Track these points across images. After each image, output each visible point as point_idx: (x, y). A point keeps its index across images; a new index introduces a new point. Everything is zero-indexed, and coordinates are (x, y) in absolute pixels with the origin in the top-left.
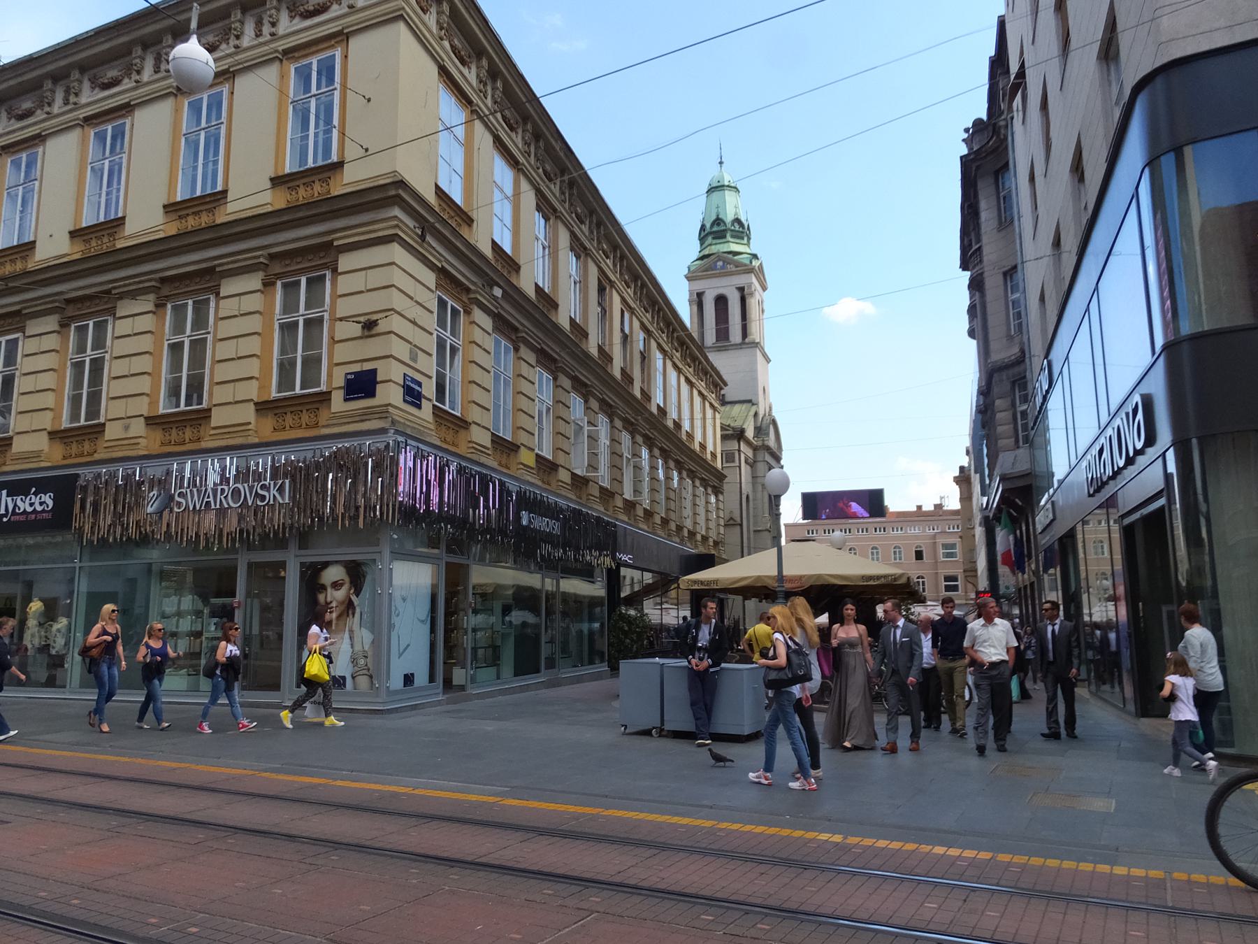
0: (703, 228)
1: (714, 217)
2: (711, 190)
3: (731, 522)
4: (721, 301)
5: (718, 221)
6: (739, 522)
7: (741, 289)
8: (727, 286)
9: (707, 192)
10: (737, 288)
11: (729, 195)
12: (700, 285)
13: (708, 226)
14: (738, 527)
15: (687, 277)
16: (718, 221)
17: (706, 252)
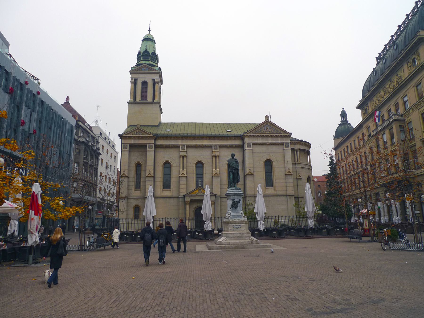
0: (139, 53)
2: (144, 40)
4: (145, 83)
5: (146, 51)
6: (153, 176)
7: (154, 80)
8: (148, 78)
12: (136, 76)
13: (142, 52)
14: (153, 178)
15: (131, 73)
16: (146, 51)
17: (139, 63)
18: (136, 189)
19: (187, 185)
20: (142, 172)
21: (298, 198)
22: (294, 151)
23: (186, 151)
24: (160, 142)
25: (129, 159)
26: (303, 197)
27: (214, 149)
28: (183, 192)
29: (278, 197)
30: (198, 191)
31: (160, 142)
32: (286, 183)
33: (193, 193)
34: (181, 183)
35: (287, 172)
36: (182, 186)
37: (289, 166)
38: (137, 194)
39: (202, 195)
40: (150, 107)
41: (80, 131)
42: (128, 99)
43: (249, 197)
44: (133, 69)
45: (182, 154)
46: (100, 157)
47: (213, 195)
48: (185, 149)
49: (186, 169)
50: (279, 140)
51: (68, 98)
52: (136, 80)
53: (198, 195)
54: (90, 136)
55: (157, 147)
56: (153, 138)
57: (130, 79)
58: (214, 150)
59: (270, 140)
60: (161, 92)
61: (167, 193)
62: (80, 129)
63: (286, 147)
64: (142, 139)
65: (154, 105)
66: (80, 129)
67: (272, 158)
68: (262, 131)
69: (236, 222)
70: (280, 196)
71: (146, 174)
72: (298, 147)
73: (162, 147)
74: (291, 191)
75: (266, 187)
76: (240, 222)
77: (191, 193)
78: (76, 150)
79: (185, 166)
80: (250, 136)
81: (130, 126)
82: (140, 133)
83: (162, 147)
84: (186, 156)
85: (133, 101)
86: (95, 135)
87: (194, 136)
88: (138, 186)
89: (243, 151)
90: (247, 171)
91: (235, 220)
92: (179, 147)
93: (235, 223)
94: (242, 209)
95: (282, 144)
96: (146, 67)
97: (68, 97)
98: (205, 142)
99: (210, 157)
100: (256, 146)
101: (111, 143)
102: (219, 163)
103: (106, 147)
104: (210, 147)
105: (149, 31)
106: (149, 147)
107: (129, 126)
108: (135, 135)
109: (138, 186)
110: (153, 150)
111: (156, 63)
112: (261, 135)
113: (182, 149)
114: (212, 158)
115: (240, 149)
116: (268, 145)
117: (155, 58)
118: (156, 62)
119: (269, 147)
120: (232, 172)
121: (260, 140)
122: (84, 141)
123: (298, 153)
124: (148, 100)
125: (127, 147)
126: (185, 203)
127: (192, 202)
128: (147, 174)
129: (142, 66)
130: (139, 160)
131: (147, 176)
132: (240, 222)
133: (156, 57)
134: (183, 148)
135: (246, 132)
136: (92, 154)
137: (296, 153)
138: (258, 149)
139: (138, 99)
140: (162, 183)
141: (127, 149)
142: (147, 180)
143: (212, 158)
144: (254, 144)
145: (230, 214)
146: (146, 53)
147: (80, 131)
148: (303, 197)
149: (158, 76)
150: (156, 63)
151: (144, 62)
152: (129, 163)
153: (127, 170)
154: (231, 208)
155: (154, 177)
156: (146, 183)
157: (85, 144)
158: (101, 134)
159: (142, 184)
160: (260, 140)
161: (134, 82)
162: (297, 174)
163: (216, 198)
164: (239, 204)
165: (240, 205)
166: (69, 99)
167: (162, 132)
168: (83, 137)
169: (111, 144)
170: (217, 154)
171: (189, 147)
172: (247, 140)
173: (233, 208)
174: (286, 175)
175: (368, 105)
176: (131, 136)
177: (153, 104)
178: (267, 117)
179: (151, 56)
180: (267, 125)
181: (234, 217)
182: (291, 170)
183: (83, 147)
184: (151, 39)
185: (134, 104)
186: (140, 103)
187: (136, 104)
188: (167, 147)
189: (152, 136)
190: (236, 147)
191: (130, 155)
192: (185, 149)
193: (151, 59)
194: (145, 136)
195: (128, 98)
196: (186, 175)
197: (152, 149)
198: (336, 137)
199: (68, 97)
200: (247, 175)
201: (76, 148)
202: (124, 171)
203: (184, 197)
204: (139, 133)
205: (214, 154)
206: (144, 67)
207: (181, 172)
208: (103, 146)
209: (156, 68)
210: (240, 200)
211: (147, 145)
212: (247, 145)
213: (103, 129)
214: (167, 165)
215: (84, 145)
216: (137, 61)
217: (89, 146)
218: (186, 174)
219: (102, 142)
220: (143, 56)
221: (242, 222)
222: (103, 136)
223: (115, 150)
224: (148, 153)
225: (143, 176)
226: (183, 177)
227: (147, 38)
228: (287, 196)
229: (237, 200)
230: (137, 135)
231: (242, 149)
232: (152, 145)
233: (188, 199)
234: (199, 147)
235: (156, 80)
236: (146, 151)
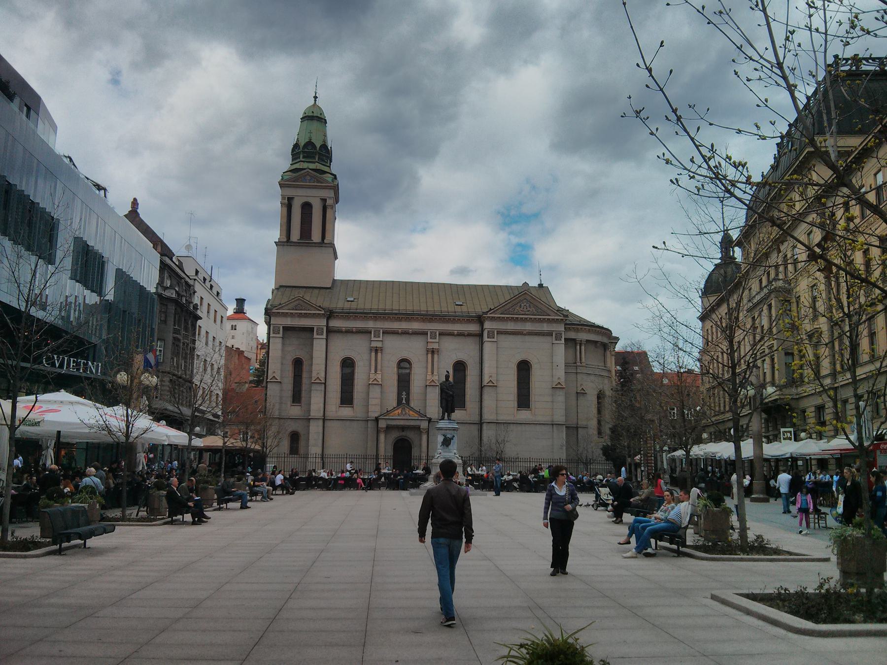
0: (296, 146)
1: (307, 140)
3: (318, 381)
4: (307, 207)
5: (310, 144)
8: (314, 197)
12: (290, 192)
13: (302, 144)
14: (323, 385)
16: (310, 144)
17: (297, 166)
18: (293, 402)
19: (382, 399)
20: (305, 375)
21: (577, 428)
22: (576, 344)
24: (335, 323)
25: (283, 350)
26: (587, 428)
27: (431, 338)
28: (374, 412)
29: (538, 427)
30: (400, 411)
31: (335, 323)
32: (552, 402)
33: (391, 414)
35: (556, 383)
36: (372, 402)
37: (560, 373)
38: (295, 411)
40: (316, 251)
44: (285, 178)
45: (374, 344)
46: (199, 322)
47: (426, 418)
48: (379, 337)
50: (545, 327)
51: (135, 203)
52: (290, 199)
55: (330, 331)
58: (429, 340)
59: (529, 327)
61: (346, 412)
63: (556, 340)
67: (529, 358)
68: (516, 311)
71: (311, 378)
72: (583, 336)
73: (339, 331)
74: (560, 417)
79: (379, 367)
81: (281, 286)
83: (339, 331)
84: (381, 349)
85: (285, 240)
86: (188, 276)
87: (396, 314)
88: (297, 398)
90: (486, 380)
94: (456, 448)
95: (550, 334)
96: (309, 176)
97: (135, 200)
98: (416, 326)
99: (424, 352)
101: (213, 289)
102: (438, 361)
103: (208, 299)
104: (424, 333)
105: (316, 97)
107: (280, 288)
108: (293, 309)
109: (297, 398)
110: (324, 336)
111: (328, 165)
113: (374, 337)
114: (427, 354)
115: (477, 339)
116: (525, 335)
118: (327, 162)
121: (510, 326)
122: (174, 296)
123: (583, 347)
126: (378, 432)
127: (389, 428)
130: (299, 354)
133: (329, 153)
134: (377, 335)
135: (488, 312)
137: (578, 347)
138: (506, 342)
139: (295, 236)
140: (339, 395)
143: (427, 354)
144: (500, 333)
146: (310, 147)
148: (587, 428)
149: (331, 194)
151: (305, 165)
152: (283, 358)
153: (279, 372)
155: (325, 384)
157: (176, 302)
158: (197, 272)
159: (304, 394)
160: (510, 326)
161: (288, 204)
162: (579, 385)
163: (431, 423)
167: (339, 304)
169: (215, 291)
170: (436, 346)
172: (487, 325)
175: (750, 244)
179: (319, 154)
182: (562, 380)
183: (172, 308)
184: (319, 116)
185: (288, 245)
188: (349, 332)
189: (323, 312)
190: (470, 335)
191: (283, 344)
192: (379, 337)
195: (276, 234)
198: (706, 292)
199: (135, 200)
203: (377, 420)
205: (430, 346)
206: (306, 176)
208: (202, 298)
209: (329, 178)
210: (454, 436)
213: (200, 260)
214: (348, 364)
216: (293, 160)
218: (380, 380)
219: (200, 291)
222: (201, 276)
223: (220, 302)
224: (315, 342)
225: (305, 381)
226: (375, 386)
227: (311, 114)
228: (553, 425)
229: (449, 436)
230: (296, 310)
232: (323, 329)
233: (382, 424)
234: (405, 333)
235: (329, 202)
236: (313, 339)
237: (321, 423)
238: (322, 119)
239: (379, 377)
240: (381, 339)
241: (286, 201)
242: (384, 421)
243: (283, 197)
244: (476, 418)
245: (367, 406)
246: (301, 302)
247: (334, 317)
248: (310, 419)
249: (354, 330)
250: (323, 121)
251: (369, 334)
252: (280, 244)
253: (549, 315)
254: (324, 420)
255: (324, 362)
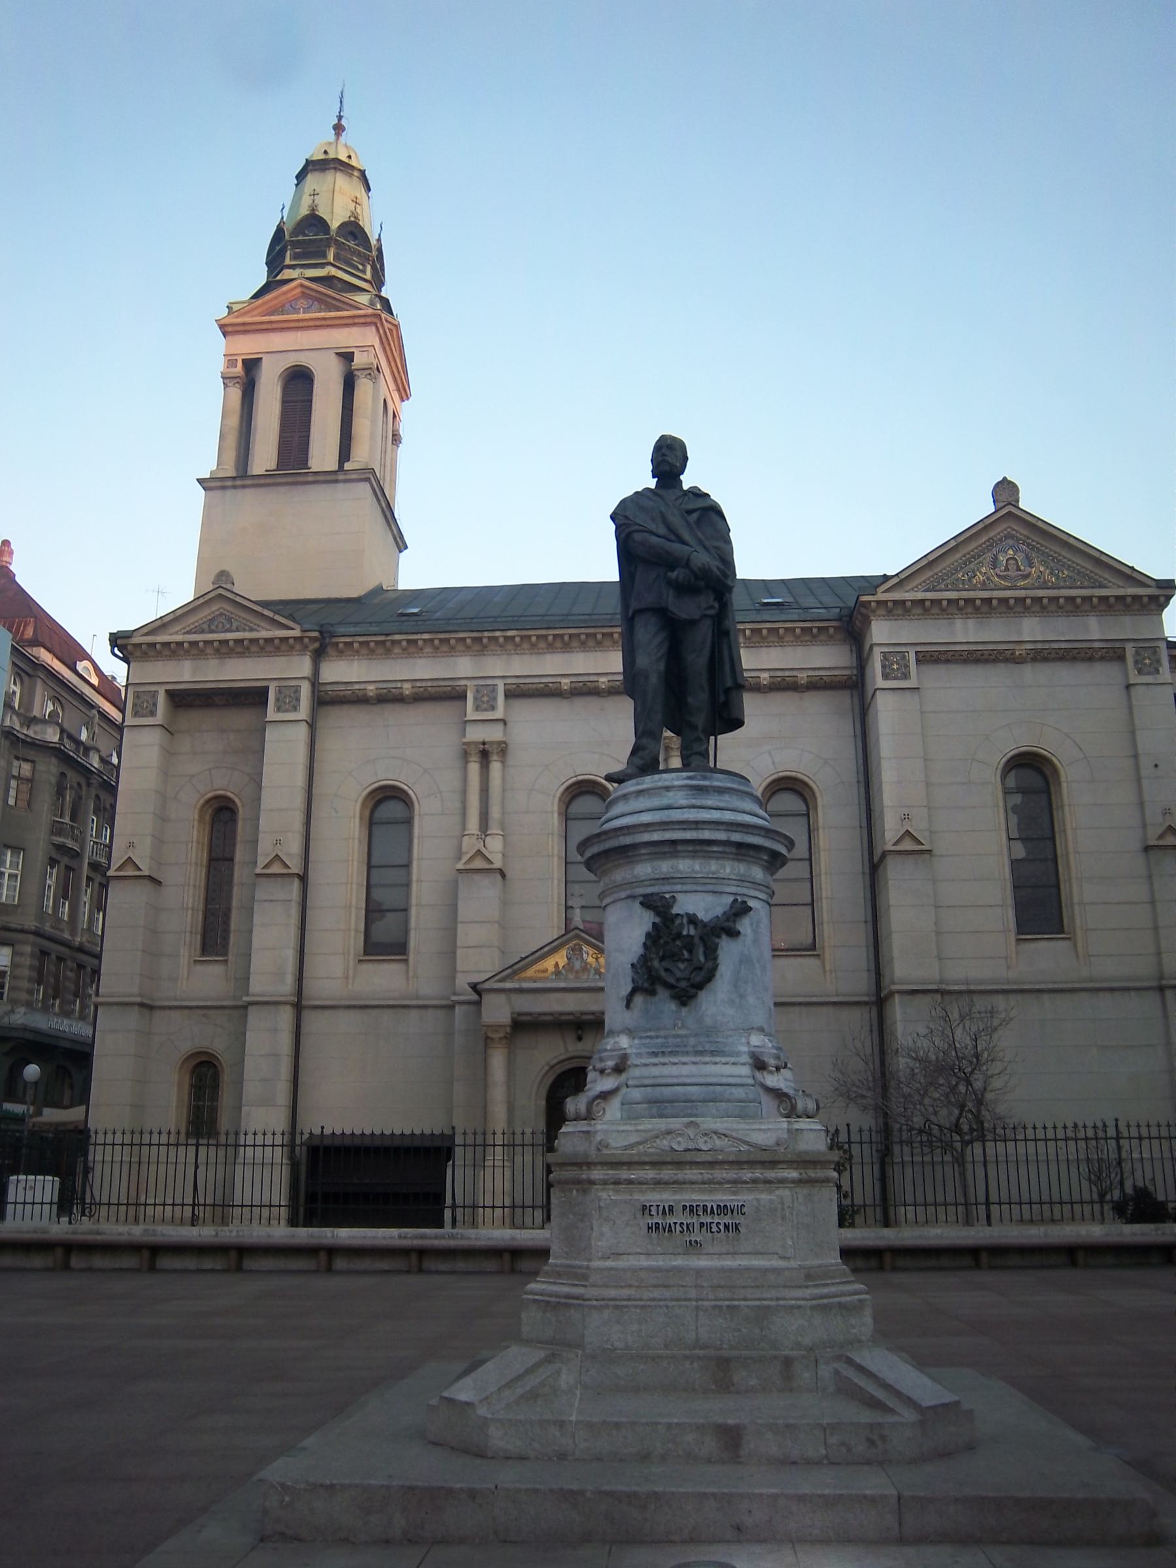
0: (279, 233)
2: (311, 167)
3: (276, 869)
7: (347, 357)
9: (297, 177)
10: (336, 353)
11: (343, 184)
12: (249, 345)
14: (296, 884)
15: (226, 329)
16: (314, 221)
20: (240, 854)
23: (504, 722)
25: (165, 773)
33: (530, 972)
34: (463, 912)
35: (1160, 830)
36: (468, 935)
39: (593, 985)
40: (319, 495)
41: (39, 690)
42: (208, 465)
43: (907, 998)
44: (236, 307)
45: (476, 734)
48: (493, 708)
49: (503, 825)
52: (252, 365)
53: (562, 985)
54: (97, 719)
56: (306, 647)
57: (220, 365)
60: (396, 439)
62: (39, 683)
64: (241, 655)
65: (340, 486)
66: (39, 683)
69: (679, 1164)
70: (1112, 990)
73: (355, 699)
75: (1019, 933)
76: (737, 1164)
77: (515, 969)
78: (13, 783)
79: (495, 812)
80: (898, 610)
82: (229, 620)
83: (355, 699)
84: (503, 749)
89: (857, 709)
90: (890, 829)
91: (665, 1143)
92: (459, 696)
93: (667, 1174)
100: (941, 670)
105: (339, 129)
106: (277, 700)
108: (203, 632)
110: (303, 712)
112: (970, 601)
113: (477, 708)
115: (844, 699)
117: (359, 254)
118: (364, 272)
119: (1028, 672)
120: (662, 612)
124: (310, 464)
125: (155, 705)
128: (262, 861)
129: (285, 293)
131: (258, 870)
132: (737, 1164)
136: (105, 809)
141: (153, 713)
142: (260, 894)
144: (930, 657)
145: (619, 1069)
147: (39, 690)
149: (369, 336)
150: (368, 276)
153: (148, 841)
154: (639, 999)
155: (303, 878)
156: (257, 919)
164: (728, 950)
165: (745, 960)
166: (11, 553)
168: (53, 719)
171: (516, 693)
172: (881, 632)
173: (652, 992)
174: (1147, 849)
176: (179, 638)
177: (336, 481)
178: (1005, 491)
179: (336, 242)
180: (1009, 536)
181: (660, 1106)
184: (346, 160)
185: (234, 487)
186: (268, 481)
187: (244, 487)
188: (389, 698)
189: (297, 633)
190: (817, 685)
191: (169, 754)
192: (493, 708)
193: (336, 257)
194: (254, 635)
196: (498, 864)
197: (295, 708)
200: (884, 855)
201: (14, 777)
202: (131, 845)
204: (222, 619)
207: (470, 845)
210: (740, 910)
211: (267, 688)
212: (884, 667)
215: (54, 760)
217: (86, 771)
220: (295, 244)
221: (752, 1164)
224: (271, 734)
225: (240, 873)
226: (477, 877)
227: (322, 157)
230: (212, 632)
231: (856, 700)
232: (297, 690)
233: (498, 1012)
235: (359, 360)
237: (286, 1016)
238: (353, 168)
239: (495, 845)
240: (499, 713)
241: (239, 369)
242: (501, 999)
243: (231, 363)
244: (859, 984)
245: (450, 953)
246: (228, 607)
247: (341, 653)
248: (245, 1007)
249: (407, 689)
250: (356, 173)
251: (458, 704)
252: (212, 484)
253: (1101, 586)
254: (298, 1007)
255: (299, 801)
